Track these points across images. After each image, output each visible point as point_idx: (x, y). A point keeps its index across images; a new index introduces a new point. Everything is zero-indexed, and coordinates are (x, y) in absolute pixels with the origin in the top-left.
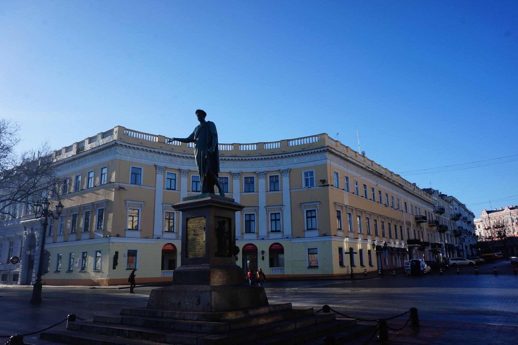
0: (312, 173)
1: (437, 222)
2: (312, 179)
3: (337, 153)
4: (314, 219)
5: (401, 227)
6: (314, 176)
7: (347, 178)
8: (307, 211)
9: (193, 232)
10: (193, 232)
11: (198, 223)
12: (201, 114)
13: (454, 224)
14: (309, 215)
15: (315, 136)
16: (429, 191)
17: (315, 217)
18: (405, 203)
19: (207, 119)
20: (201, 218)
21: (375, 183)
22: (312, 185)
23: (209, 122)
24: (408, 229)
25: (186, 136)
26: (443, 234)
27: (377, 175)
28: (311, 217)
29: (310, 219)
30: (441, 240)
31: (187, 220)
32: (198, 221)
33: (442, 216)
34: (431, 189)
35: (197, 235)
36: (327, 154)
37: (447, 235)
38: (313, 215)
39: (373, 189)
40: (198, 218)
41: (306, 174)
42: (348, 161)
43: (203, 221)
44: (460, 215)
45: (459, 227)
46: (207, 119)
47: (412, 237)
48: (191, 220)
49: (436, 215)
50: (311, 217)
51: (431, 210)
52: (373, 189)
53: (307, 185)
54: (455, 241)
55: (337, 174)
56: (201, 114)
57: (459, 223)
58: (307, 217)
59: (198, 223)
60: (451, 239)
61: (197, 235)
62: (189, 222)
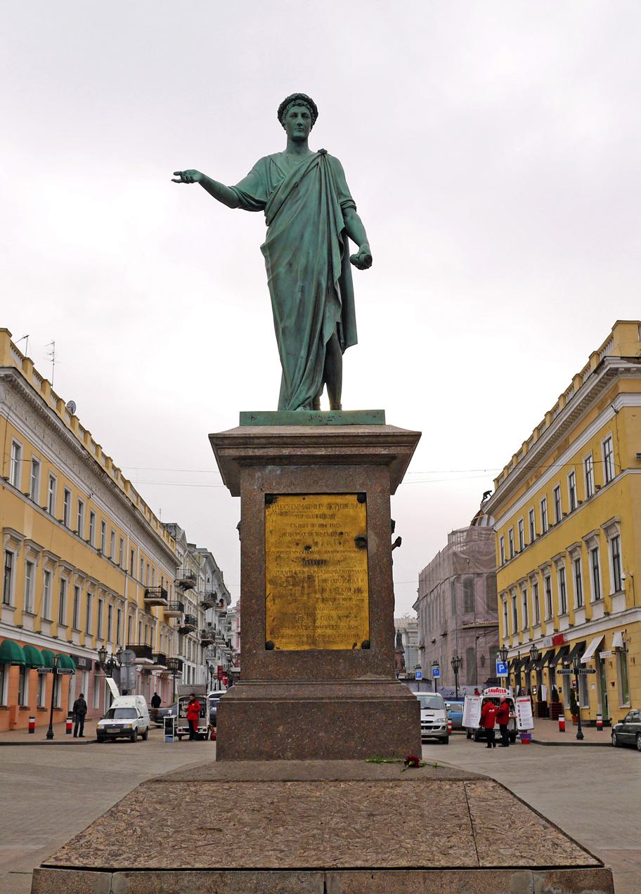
1: (181, 607)
3: (28, 390)
7: (35, 464)
9: (298, 552)
10: (298, 552)
11: (324, 516)
12: (298, 113)
13: (202, 614)
18: (132, 552)
19: (315, 142)
20: (339, 500)
21: (87, 491)
23: (323, 153)
24: (130, 617)
26: (184, 637)
27: (92, 471)
30: (180, 654)
31: (270, 499)
32: (324, 510)
33: (187, 594)
34: (175, 526)
35: (320, 563)
37: (190, 639)
39: (81, 504)
40: (326, 500)
42: (44, 419)
43: (351, 512)
44: (214, 596)
45: (210, 624)
47: (135, 642)
49: (177, 590)
52: (81, 504)
55: (18, 448)
56: (298, 113)
57: (210, 616)
59: (324, 516)
60: (194, 648)
61: (320, 563)
62: (274, 508)
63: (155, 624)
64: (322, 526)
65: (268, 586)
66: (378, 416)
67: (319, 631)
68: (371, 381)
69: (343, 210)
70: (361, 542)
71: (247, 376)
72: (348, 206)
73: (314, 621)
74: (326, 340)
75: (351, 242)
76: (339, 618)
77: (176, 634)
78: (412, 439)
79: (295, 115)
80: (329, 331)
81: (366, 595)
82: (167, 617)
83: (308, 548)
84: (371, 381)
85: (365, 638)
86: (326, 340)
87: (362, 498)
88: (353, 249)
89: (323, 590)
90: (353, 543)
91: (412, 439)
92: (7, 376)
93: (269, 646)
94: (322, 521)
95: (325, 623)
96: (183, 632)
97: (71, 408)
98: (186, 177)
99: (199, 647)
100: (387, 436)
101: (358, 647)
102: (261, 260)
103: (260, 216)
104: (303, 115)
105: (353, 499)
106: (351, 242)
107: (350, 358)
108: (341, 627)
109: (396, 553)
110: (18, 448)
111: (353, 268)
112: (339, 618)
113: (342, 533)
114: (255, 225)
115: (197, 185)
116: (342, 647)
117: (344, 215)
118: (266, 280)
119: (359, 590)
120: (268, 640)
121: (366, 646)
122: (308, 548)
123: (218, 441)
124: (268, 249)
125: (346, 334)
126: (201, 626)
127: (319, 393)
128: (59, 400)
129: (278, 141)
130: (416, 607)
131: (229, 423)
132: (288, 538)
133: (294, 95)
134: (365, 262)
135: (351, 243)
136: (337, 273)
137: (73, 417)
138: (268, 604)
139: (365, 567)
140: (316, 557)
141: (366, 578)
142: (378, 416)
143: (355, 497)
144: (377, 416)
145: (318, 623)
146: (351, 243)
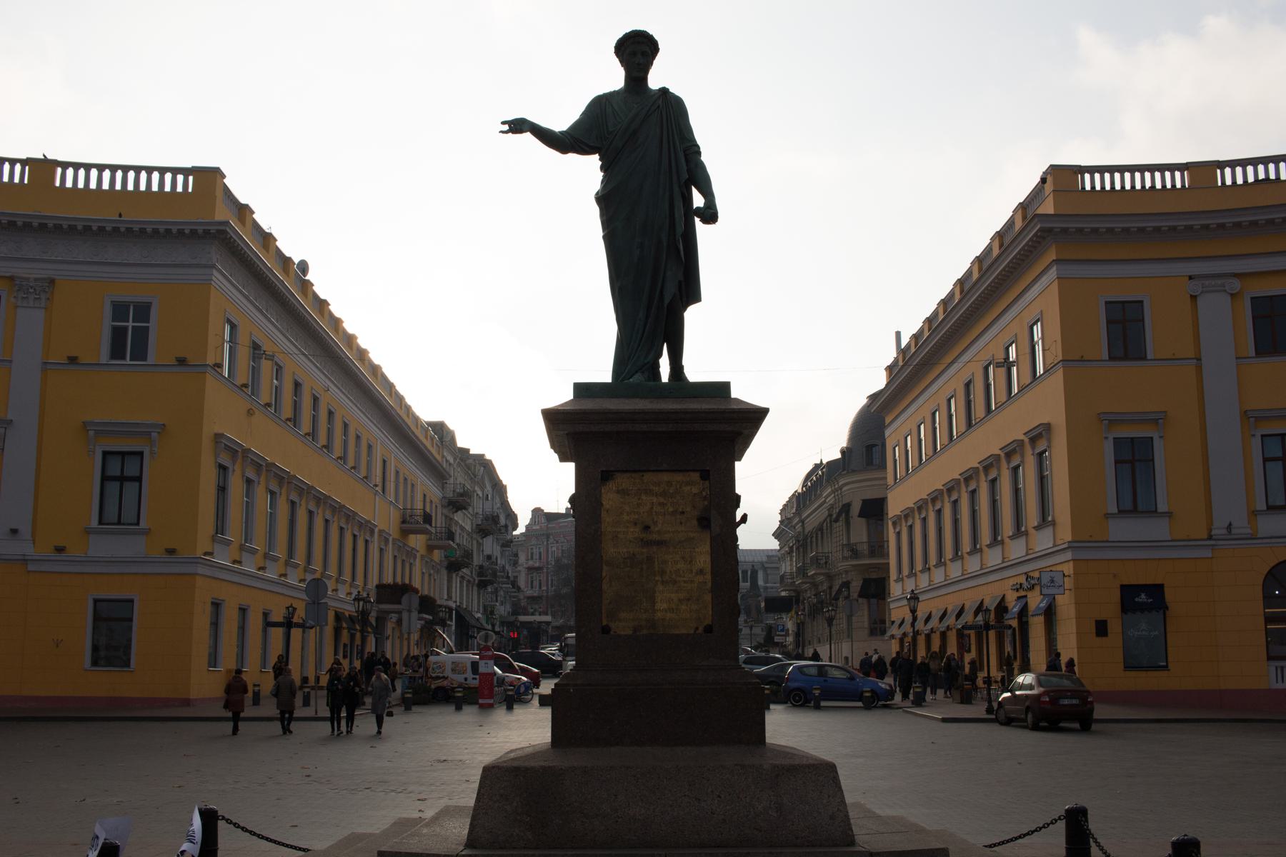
0: (143, 311)
1: (451, 536)
2: (142, 336)
4: (130, 488)
5: (367, 541)
6: (152, 325)
8: (105, 454)
12: (637, 50)
13: (479, 544)
14: (114, 470)
15: (175, 171)
16: (440, 430)
17: (139, 479)
19: (655, 80)
20: (679, 477)
22: (140, 352)
23: (664, 91)
24: (381, 550)
25: (561, 122)
28: (122, 479)
29: (113, 487)
30: (450, 598)
31: (606, 476)
33: (458, 517)
36: (214, 254)
37: (462, 577)
38: (131, 470)
40: (665, 477)
41: (120, 310)
45: (489, 557)
46: (655, 80)
48: (623, 481)
49: (445, 511)
50: (122, 479)
51: (435, 492)
52: (316, 399)
53: (117, 351)
54: (475, 602)
56: (637, 50)
57: (490, 546)
58: (105, 478)
61: (660, 543)
62: (611, 485)
63: (415, 558)
64: (660, 504)
65: (605, 568)
66: (724, 388)
67: (659, 615)
68: (711, 348)
69: (686, 156)
70: (704, 522)
71: (584, 343)
72: (692, 151)
73: (654, 603)
74: (667, 301)
75: (694, 191)
76: (680, 600)
77: (444, 572)
78: (756, 416)
79: (634, 54)
80: (670, 290)
81: (709, 577)
82: (430, 548)
83: (647, 528)
84: (711, 348)
85: (708, 622)
86: (667, 301)
87: (705, 475)
88: (698, 200)
89: (663, 573)
90: (695, 522)
91: (756, 416)
92: (218, 231)
93: (606, 630)
94: (662, 500)
95: (665, 606)
96: (453, 567)
97: (304, 266)
98: (517, 126)
99: (475, 588)
100: (734, 411)
101: (701, 630)
102: (596, 210)
103: (594, 161)
104: (644, 54)
105: (697, 474)
106: (694, 191)
107: (692, 315)
108: (677, 604)
109: (740, 531)
110: (233, 327)
111: (697, 220)
112: (680, 600)
113: (683, 513)
114: (587, 171)
115: (528, 136)
116: (684, 631)
117: (687, 161)
118: (601, 234)
119: (701, 572)
120: (605, 623)
121: (708, 629)
122: (647, 528)
123: (553, 418)
124: (603, 199)
125: (691, 293)
126: (477, 560)
127: (660, 355)
128: (287, 261)
129: (613, 78)
130: (777, 535)
131: (562, 395)
132: (626, 517)
133: (633, 32)
134: (710, 215)
135: (695, 192)
136: (680, 229)
137: (306, 286)
138: (605, 587)
139: (708, 548)
140: (655, 537)
141: (708, 559)
142: (724, 388)
143: (697, 474)
144: (722, 389)
145: (658, 606)
146: (695, 192)
